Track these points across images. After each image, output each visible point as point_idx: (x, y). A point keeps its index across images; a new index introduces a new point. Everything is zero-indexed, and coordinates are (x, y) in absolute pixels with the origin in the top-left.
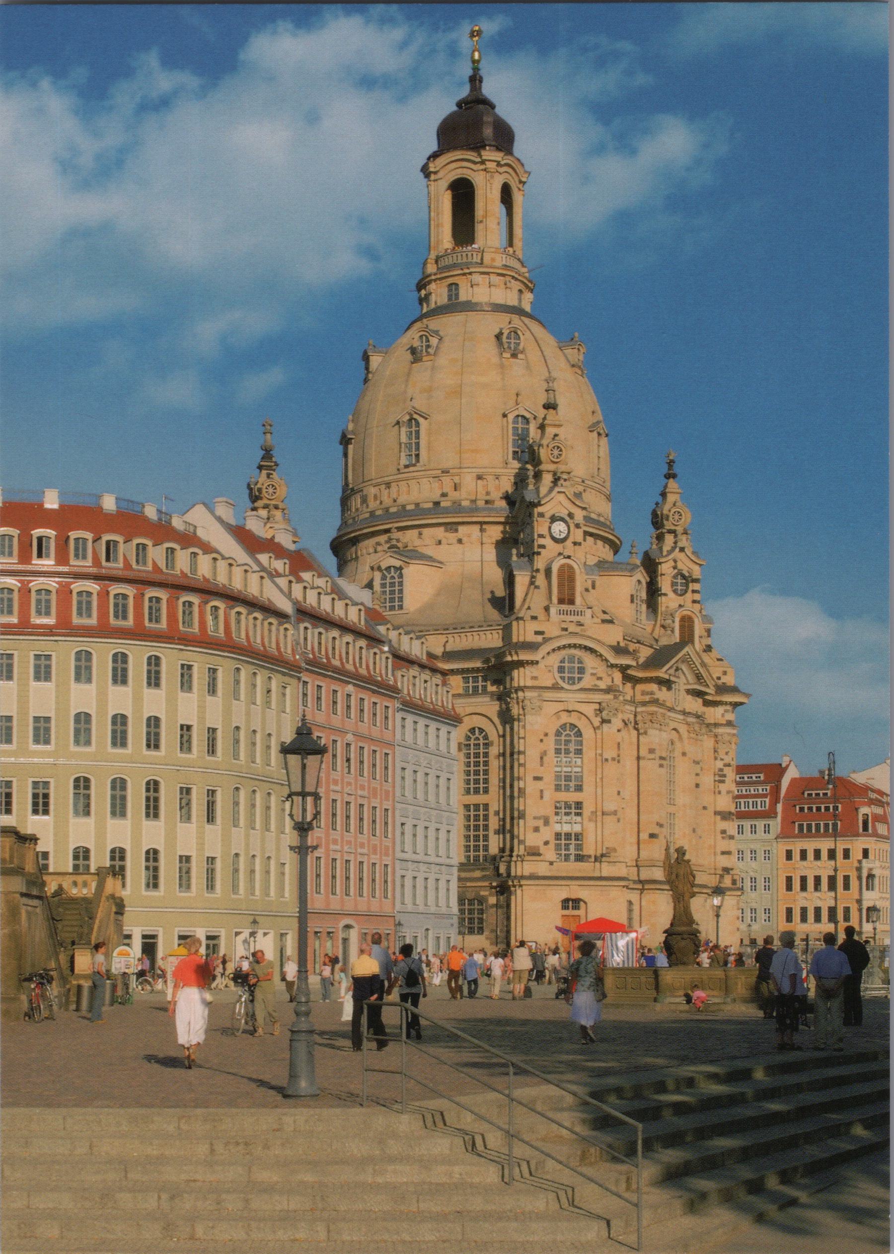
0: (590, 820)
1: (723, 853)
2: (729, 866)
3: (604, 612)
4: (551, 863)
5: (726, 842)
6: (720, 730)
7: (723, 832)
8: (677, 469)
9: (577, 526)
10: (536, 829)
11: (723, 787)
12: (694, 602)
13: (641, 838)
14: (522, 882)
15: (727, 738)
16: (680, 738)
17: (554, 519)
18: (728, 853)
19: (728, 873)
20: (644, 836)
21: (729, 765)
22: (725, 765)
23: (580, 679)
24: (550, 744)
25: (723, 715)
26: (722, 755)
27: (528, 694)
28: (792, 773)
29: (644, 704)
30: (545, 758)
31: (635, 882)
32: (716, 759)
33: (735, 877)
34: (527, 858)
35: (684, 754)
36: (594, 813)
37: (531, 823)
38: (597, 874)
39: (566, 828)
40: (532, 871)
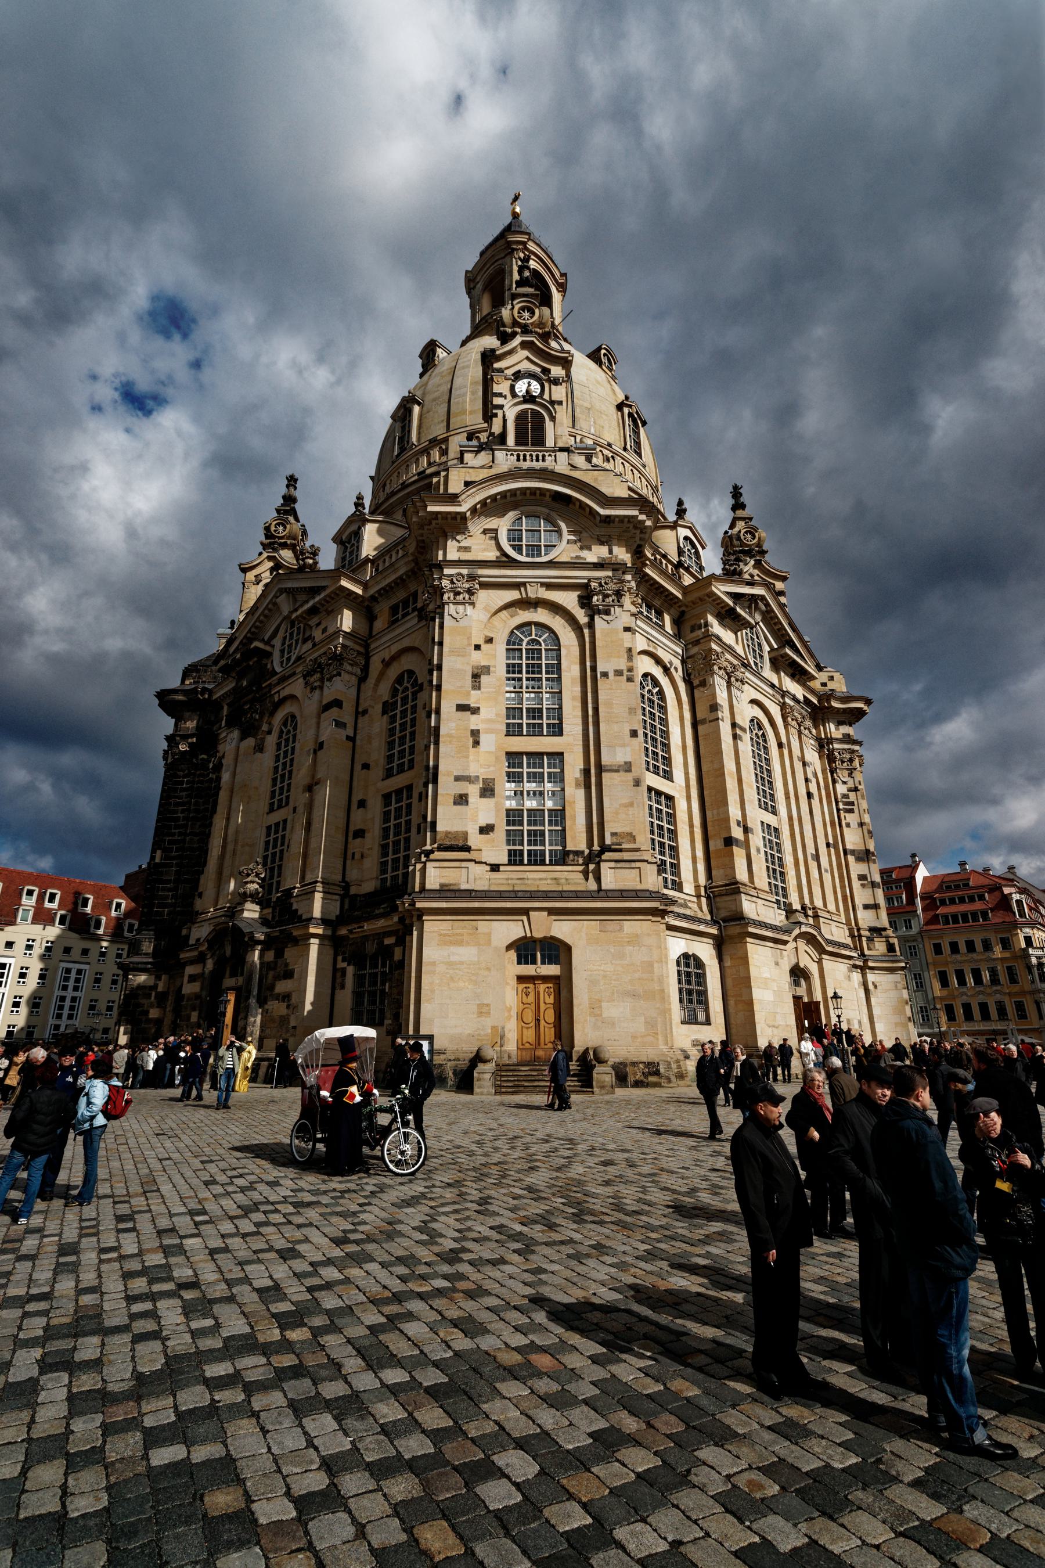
1: (866, 907)
2: (878, 925)
4: (495, 868)
5: (869, 891)
7: (862, 877)
8: (745, 499)
11: (851, 818)
13: (712, 848)
14: (419, 905)
15: (847, 756)
17: (518, 376)
18: (876, 907)
19: (881, 936)
20: (716, 844)
21: (856, 789)
22: (849, 790)
23: (550, 547)
24: (497, 657)
26: (843, 775)
27: (446, 571)
28: (921, 873)
29: (697, 642)
30: (484, 679)
32: (834, 782)
33: (891, 940)
34: (437, 855)
36: (586, 772)
37: (447, 787)
38: (592, 885)
40: (444, 881)
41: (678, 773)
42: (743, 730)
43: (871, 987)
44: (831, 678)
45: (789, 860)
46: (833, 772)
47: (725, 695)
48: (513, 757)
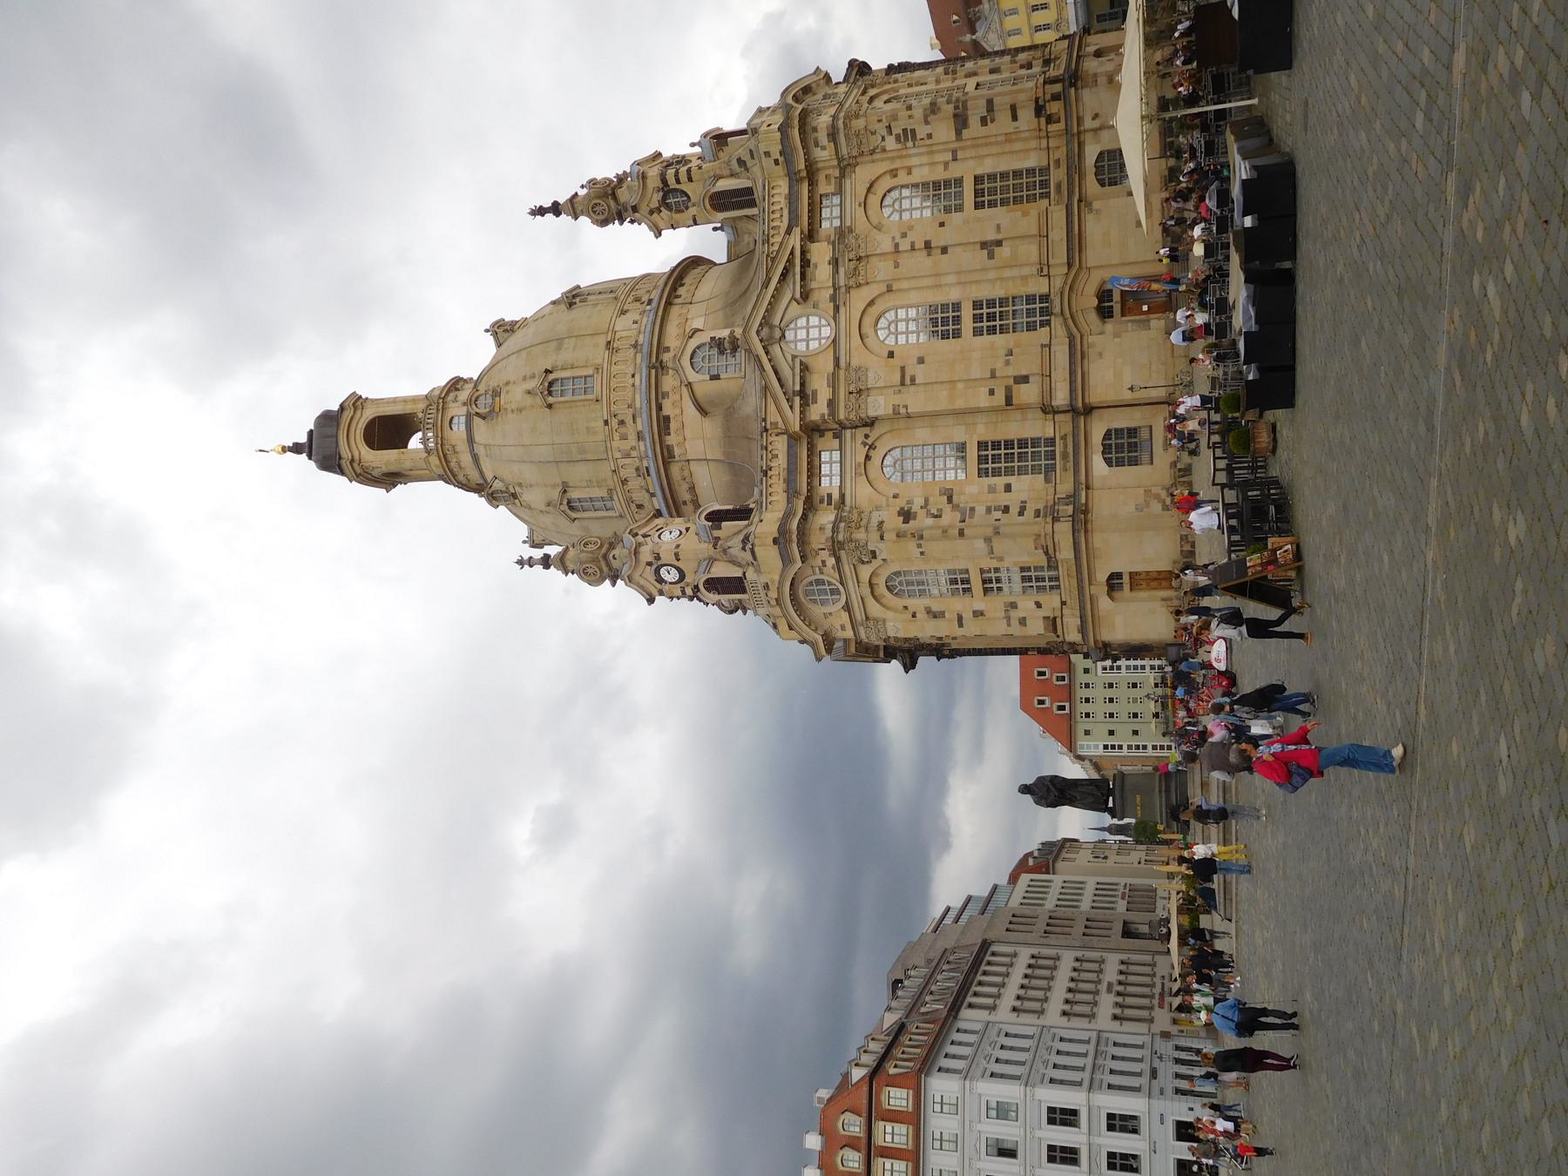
0: (1001, 559)
1: (1015, 118)
3: (744, 549)
4: (1063, 603)
5: (997, 115)
6: (844, 151)
7: (984, 121)
9: (658, 558)
10: (1023, 622)
11: (922, 131)
12: (690, 179)
16: (871, 303)
17: (660, 580)
18: (1014, 109)
21: (889, 128)
23: (830, 583)
24: (917, 604)
25: (824, 148)
30: (935, 608)
31: (1075, 428)
33: (1048, 97)
34: (1060, 632)
35: (889, 290)
37: (1016, 630)
39: (1017, 577)
41: (959, 435)
42: (903, 369)
43: (1096, 124)
44: (767, 154)
45: (998, 292)
46: (873, 152)
47: (881, 400)
48: (986, 591)
